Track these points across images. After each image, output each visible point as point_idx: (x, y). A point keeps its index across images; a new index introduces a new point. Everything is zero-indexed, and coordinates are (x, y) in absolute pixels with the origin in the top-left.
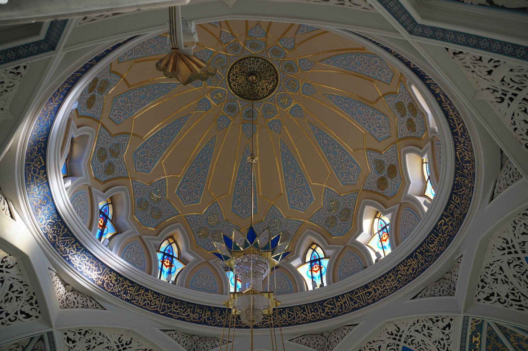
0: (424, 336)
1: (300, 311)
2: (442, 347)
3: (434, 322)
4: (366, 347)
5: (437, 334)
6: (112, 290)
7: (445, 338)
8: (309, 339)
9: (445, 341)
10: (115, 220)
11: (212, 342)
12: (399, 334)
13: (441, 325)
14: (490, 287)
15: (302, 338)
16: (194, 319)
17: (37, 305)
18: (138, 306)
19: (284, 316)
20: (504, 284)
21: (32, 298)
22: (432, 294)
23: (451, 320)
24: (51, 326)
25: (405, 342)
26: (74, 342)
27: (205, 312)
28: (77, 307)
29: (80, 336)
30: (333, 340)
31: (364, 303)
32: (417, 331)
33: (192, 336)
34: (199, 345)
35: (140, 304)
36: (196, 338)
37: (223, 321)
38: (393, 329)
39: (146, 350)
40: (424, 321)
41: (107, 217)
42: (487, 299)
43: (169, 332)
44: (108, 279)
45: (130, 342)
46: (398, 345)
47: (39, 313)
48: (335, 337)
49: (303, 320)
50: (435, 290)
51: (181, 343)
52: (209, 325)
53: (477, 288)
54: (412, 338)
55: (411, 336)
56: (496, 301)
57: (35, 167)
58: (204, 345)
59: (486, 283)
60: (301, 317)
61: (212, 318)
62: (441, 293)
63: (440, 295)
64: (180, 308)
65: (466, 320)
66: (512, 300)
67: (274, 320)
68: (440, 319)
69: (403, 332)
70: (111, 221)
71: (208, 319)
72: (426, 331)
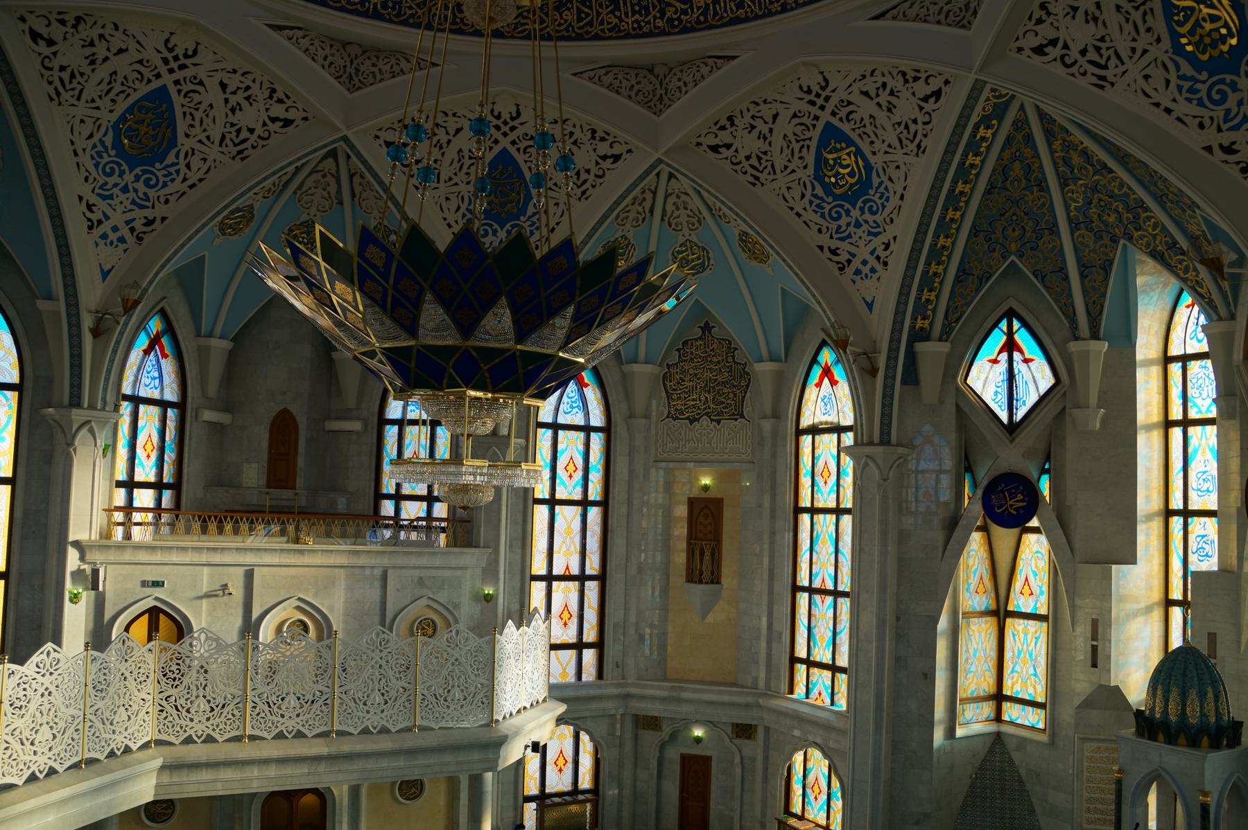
0: (877, 108)
1: (607, 7)
2: (911, 137)
3: (906, 81)
4: (745, 111)
5: (907, 108)
7: (921, 118)
8: (620, 77)
9: (920, 126)
11: (394, 61)
12: (824, 94)
13: (922, 89)
14: (1056, 24)
15: (603, 71)
19: (568, 15)
20: (1087, 22)
22: (921, 15)
23: (947, 82)
25: (834, 114)
30: (674, 84)
31: (760, 9)
32: (866, 94)
33: (345, 44)
34: (363, 68)
36: (354, 50)
38: (814, 81)
40: (886, 73)
42: (1039, 50)
43: (290, 33)
45: (195, 52)
46: (816, 118)
48: (679, 80)
49: (610, 30)
50: (931, 7)
51: (320, 60)
53: (1026, 20)
54: (851, 108)
55: (849, 103)
56: (1055, 60)
58: (373, 69)
59: (1049, 14)
60: (609, 23)
62: (942, 17)
63: (939, 22)
65: (977, 88)
66: (1090, 62)
67: (542, 21)
68: (923, 75)
69: (833, 91)
72: (884, 98)
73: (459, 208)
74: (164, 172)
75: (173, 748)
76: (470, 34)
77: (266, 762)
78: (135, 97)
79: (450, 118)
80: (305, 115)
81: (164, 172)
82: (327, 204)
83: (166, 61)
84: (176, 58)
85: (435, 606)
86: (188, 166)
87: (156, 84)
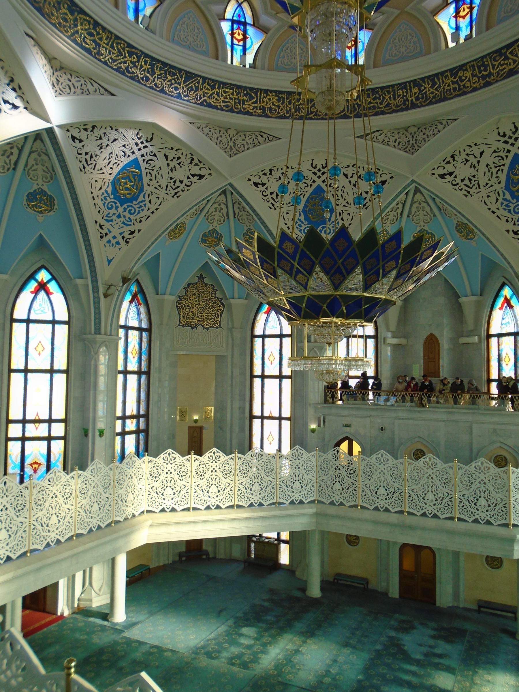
6: (278, 113)
10: (258, 21)
16: (397, 106)
17: (202, 164)
18: (318, 119)
21: (193, 159)
24: (227, 179)
26: (263, 185)
27: (411, 91)
28: (248, 149)
29: (266, 177)
34: (418, 138)
35: (319, 116)
36: (412, 130)
37: (438, 93)
39: (348, 166)
41: (245, 24)
44: (267, 103)
47: (210, 169)
52: (419, 107)
57: (86, 30)
61: (423, 95)
64: (374, 99)
70: (254, 25)
71: (417, 99)
73: (497, 200)
74: (332, 225)
75: (325, 506)
76: (470, 92)
77: (366, 521)
78: (307, 195)
79: (474, 148)
80: (391, 175)
81: (332, 225)
82: (428, 218)
83: (314, 173)
84: (319, 170)
85: (506, 447)
86: (342, 219)
87: (315, 186)
